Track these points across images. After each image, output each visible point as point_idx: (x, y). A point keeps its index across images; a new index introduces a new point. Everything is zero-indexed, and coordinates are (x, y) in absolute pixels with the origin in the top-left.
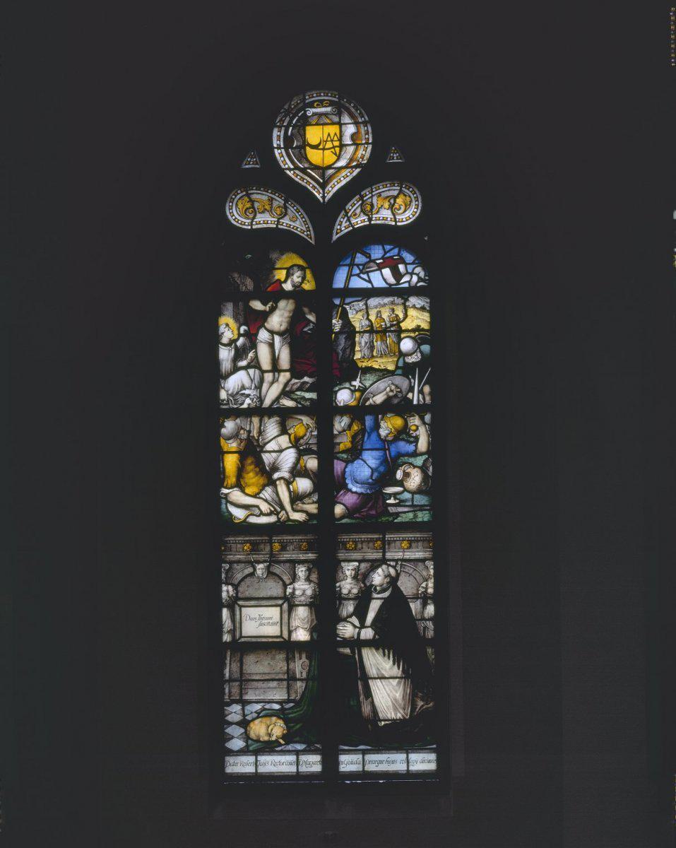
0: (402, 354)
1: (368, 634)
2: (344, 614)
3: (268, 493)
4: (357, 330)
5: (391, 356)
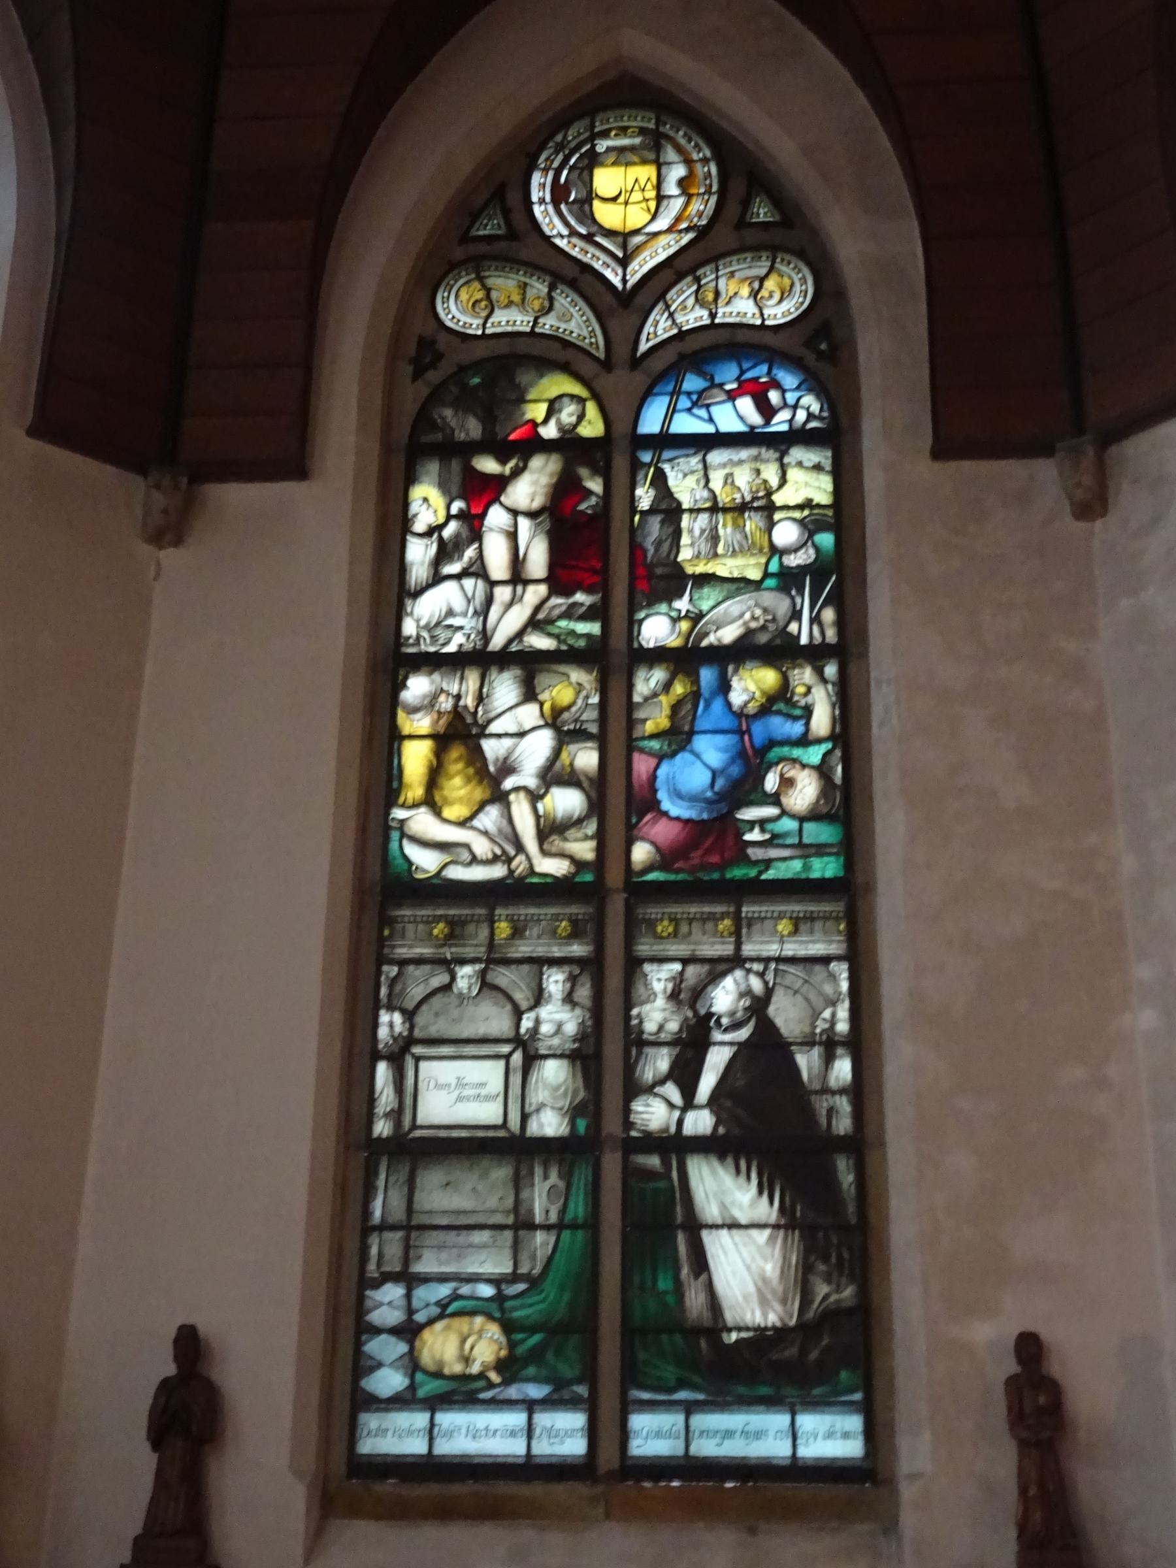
0: (774, 550)
1: (700, 1122)
2: (648, 1075)
3: (490, 818)
4: (685, 506)
5: (753, 555)
